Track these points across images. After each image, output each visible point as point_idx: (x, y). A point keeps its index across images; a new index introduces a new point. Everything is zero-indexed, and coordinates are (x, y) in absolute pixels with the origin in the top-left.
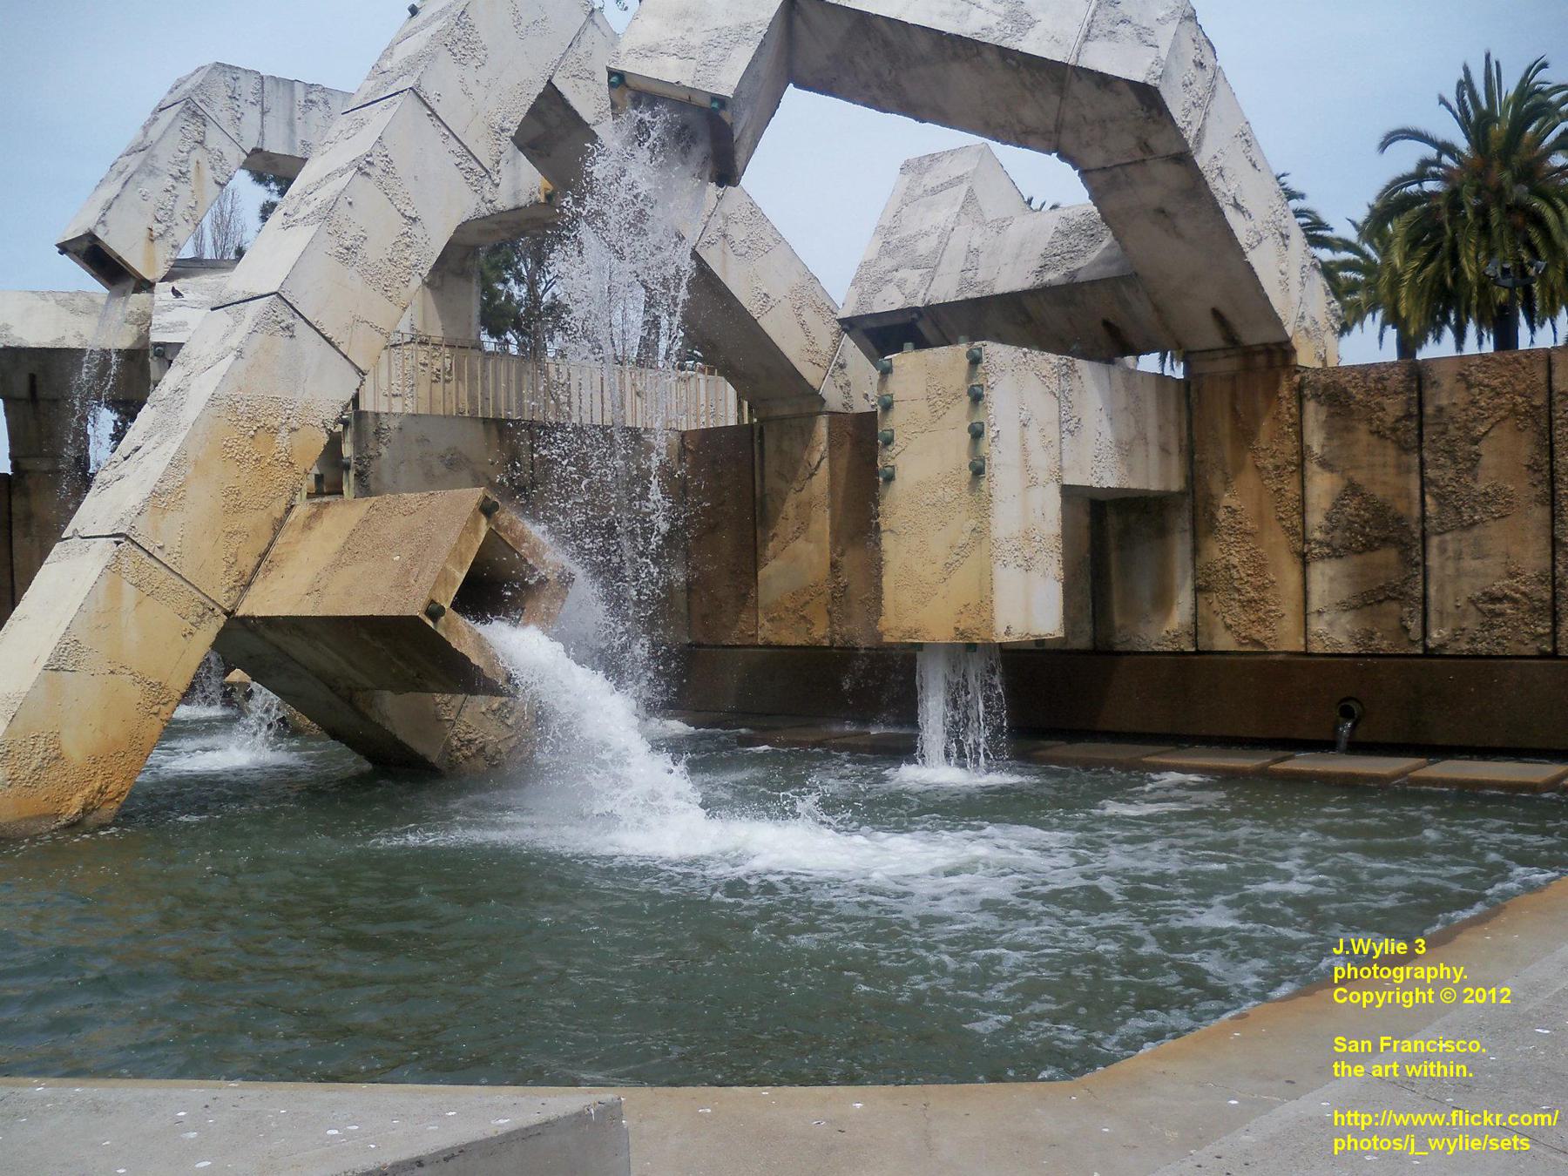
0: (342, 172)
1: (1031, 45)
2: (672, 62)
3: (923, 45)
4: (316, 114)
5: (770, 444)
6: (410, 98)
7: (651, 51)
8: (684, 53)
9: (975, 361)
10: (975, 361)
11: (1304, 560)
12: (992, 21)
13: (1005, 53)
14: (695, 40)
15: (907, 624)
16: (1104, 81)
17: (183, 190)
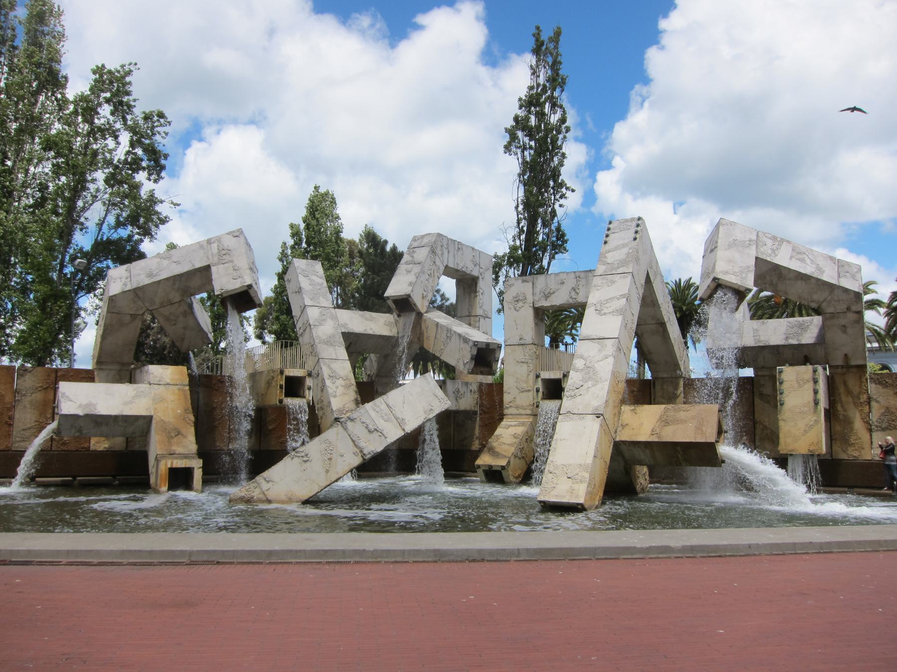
0: (618, 299)
1: (825, 278)
2: (733, 277)
3: (792, 275)
4: (460, 253)
5: (658, 387)
6: (630, 277)
7: (726, 273)
8: (734, 274)
9: (815, 371)
10: (815, 371)
11: (870, 431)
12: (813, 270)
13: (818, 280)
14: (737, 270)
15: (790, 448)
16: (846, 290)
17: (431, 280)
